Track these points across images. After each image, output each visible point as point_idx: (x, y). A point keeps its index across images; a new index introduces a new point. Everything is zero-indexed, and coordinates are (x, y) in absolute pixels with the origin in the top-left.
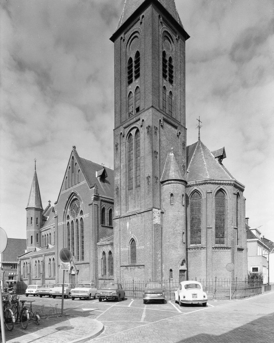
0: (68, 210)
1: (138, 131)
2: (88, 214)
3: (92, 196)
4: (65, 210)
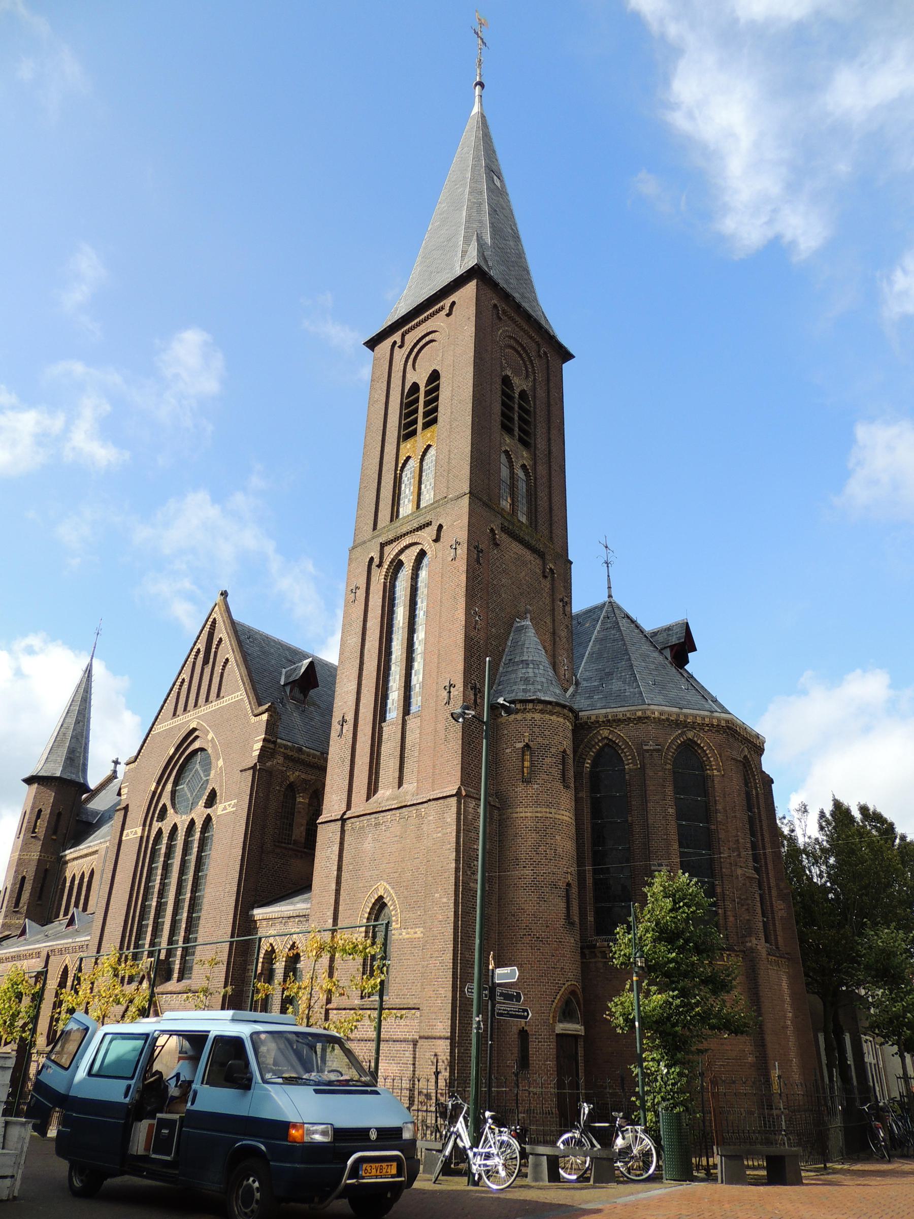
0: (169, 786)
1: (422, 554)
2: (233, 802)
3: (258, 741)
4: (156, 788)
